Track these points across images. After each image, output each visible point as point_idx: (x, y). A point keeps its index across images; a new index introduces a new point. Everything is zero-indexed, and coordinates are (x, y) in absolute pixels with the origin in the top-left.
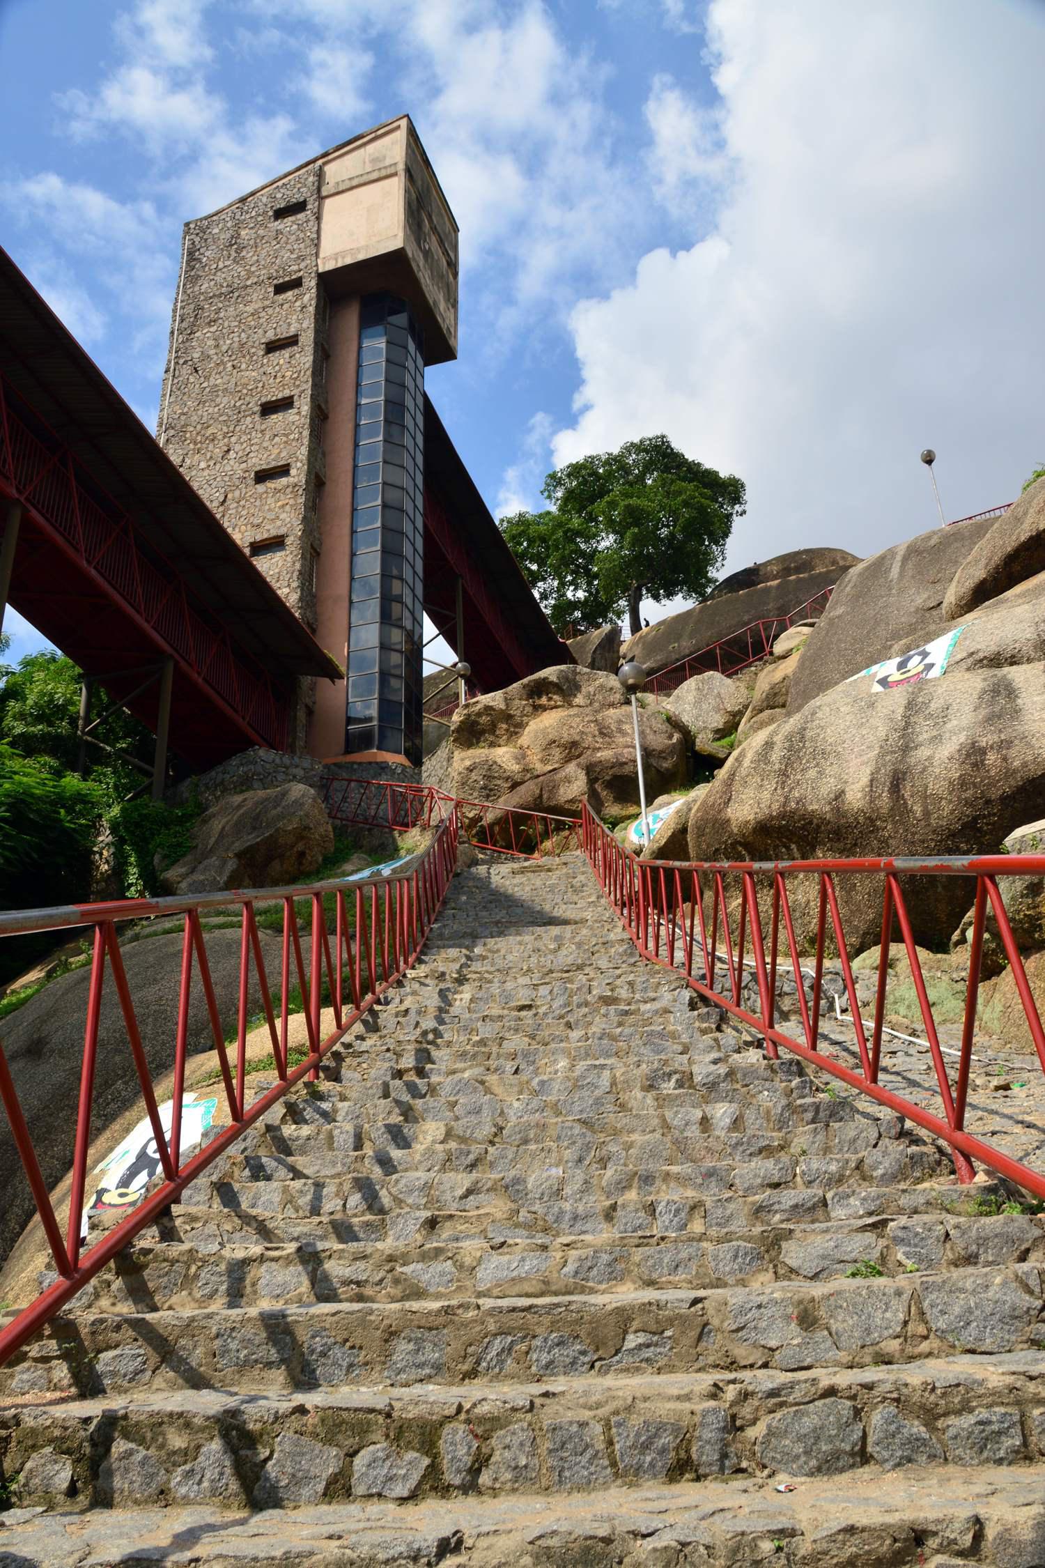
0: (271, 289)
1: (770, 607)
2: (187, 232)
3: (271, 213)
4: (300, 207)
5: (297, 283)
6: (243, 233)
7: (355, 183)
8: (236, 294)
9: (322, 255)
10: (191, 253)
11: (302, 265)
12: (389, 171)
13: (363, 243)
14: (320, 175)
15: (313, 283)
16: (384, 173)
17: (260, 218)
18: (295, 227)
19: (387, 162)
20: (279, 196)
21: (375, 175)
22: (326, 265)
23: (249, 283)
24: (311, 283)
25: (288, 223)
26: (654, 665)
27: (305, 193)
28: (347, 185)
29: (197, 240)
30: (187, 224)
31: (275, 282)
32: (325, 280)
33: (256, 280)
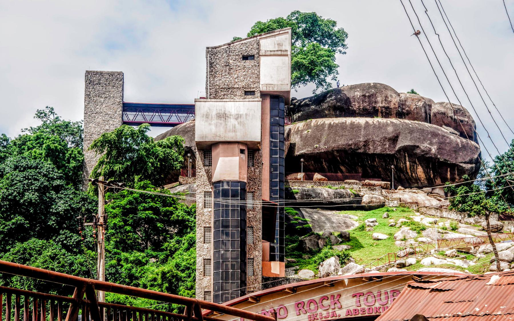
0: (243, 92)
1: (361, 139)
2: (208, 52)
3: (241, 56)
4: (252, 57)
5: (252, 93)
6: (231, 61)
7: (272, 53)
8: (230, 90)
9: (261, 83)
10: (211, 64)
11: (255, 86)
12: (285, 53)
13: (276, 83)
14: (258, 44)
15: (259, 95)
16: (283, 53)
17: (237, 57)
18: (250, 66)
19: (283, 48)
20: (244, 49)
21: (279, 53)
22: (264, 89)
23: (235, 86)
24: (258, 94)
25: (248, 63)
26: (306, 152)
27: (254, 52)
28: (269, 53)
29: (212, 57)
30: (208, 48)
31: (245, 89)
32: (261, 92)
33: (237, 86)
